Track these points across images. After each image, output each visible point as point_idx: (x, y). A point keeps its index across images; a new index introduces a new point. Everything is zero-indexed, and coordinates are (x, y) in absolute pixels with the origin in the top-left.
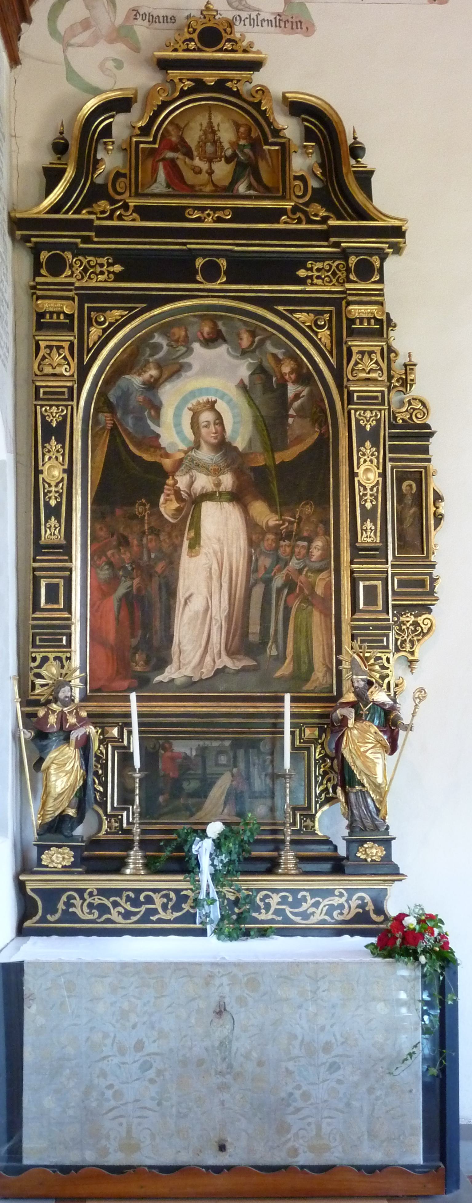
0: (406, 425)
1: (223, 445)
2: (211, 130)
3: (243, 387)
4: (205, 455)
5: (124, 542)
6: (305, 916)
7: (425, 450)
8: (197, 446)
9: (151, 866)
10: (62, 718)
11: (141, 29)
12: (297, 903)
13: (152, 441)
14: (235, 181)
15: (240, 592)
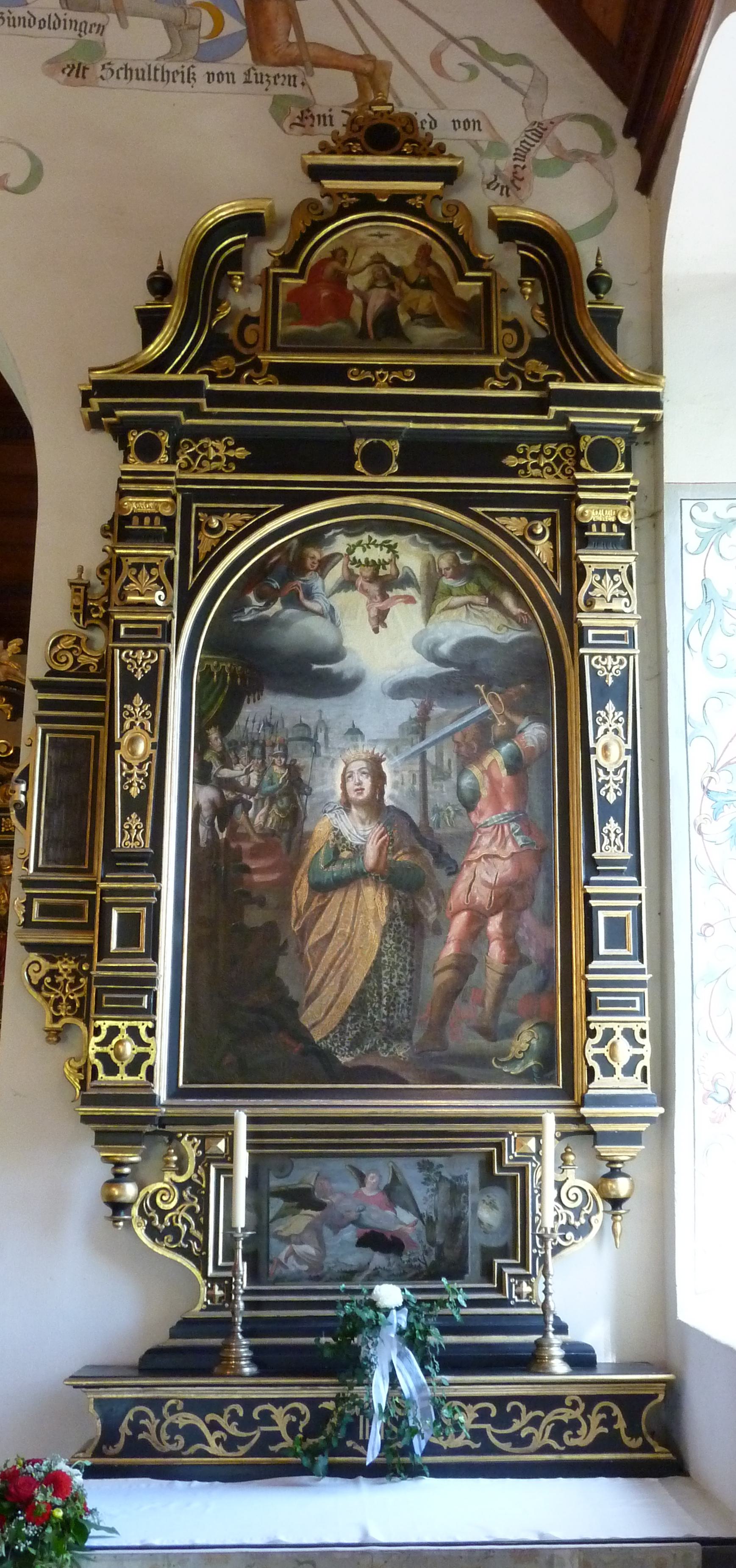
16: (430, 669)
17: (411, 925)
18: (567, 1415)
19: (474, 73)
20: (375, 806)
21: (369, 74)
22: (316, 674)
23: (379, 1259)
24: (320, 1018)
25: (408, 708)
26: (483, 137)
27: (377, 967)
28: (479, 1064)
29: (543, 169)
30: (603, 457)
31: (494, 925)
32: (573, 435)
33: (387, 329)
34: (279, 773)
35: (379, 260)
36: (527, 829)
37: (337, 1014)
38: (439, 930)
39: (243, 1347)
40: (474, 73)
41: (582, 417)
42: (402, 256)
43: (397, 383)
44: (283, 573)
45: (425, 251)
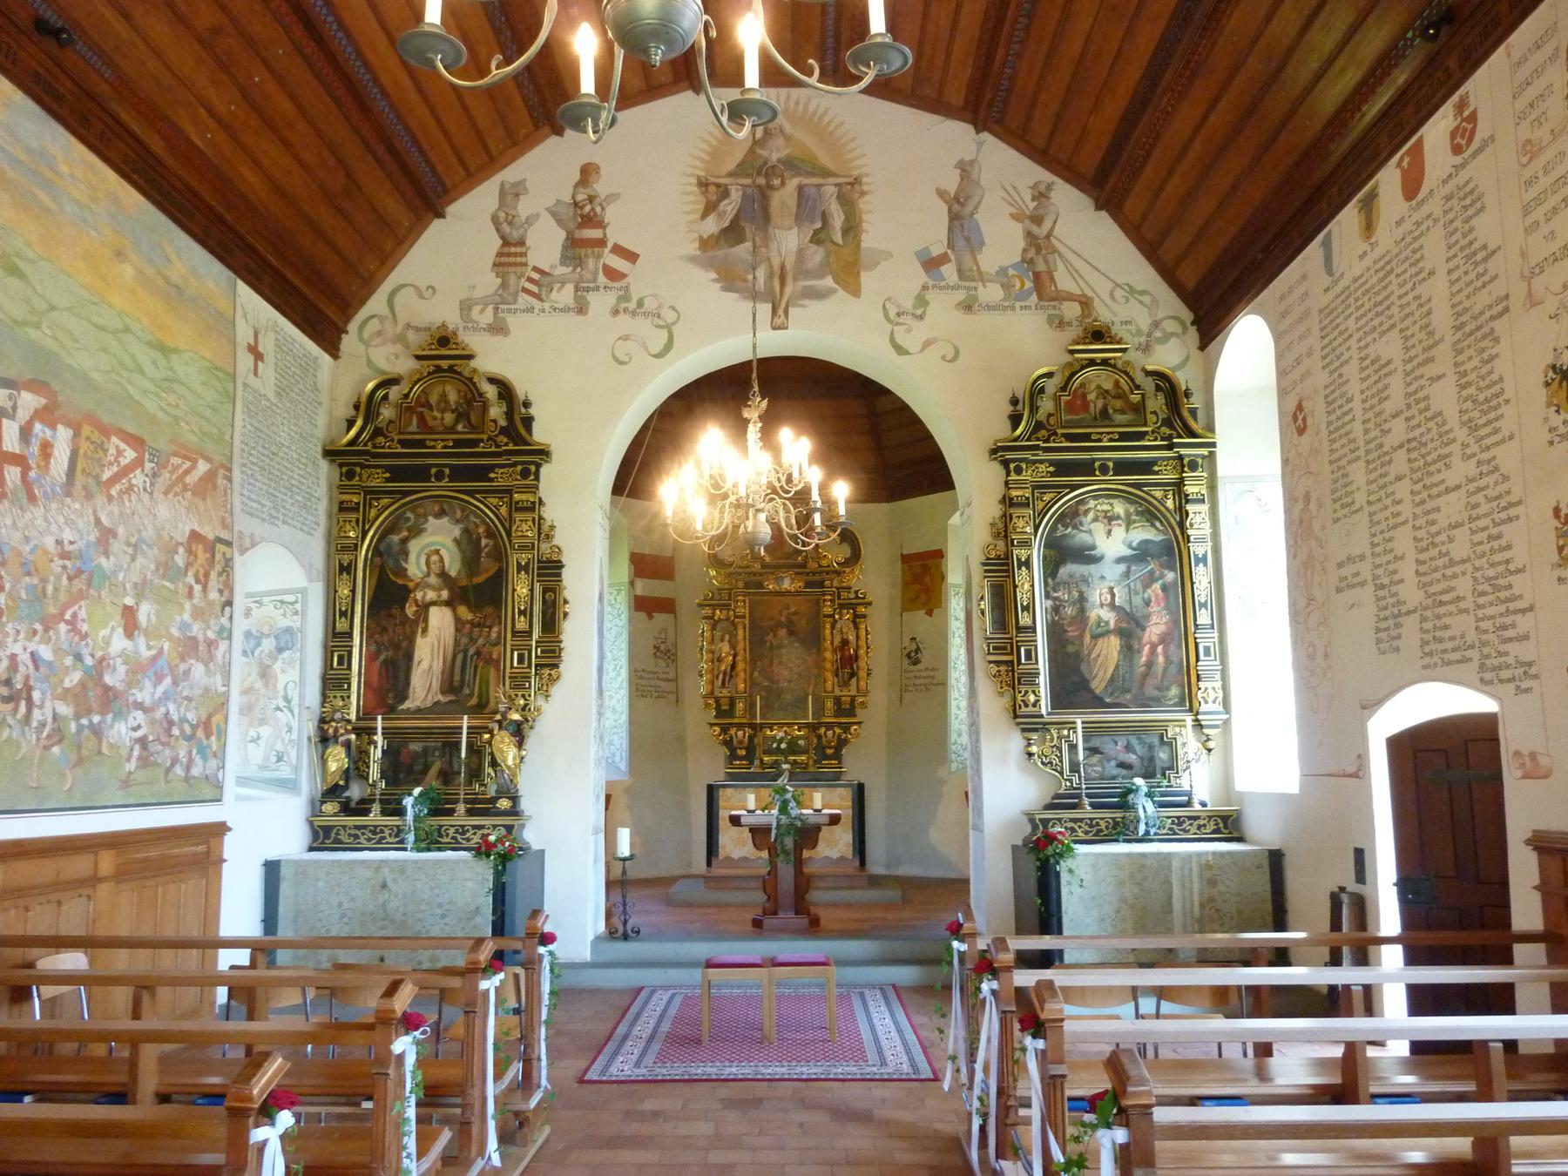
0: (549, 561)
1: (443, 574)
2: (444, 395)
3: (456, 541)
4: (433, 580)
6: (468, 840)
7: (559, 575)
8: (428, 575)
9: (384, 813)
10: (336, 730)
11: (411, 336)
12: (464, 833)
13: (402, 573)
14: (457, 422)
15: (449, 658)
16: (1130, 552)
17: (1129, 650)
18: (1202, 822)
19: (1128, 300)
20: (1112, 606)
21: (1086, 303)
22: (1086, 556)
23: (1124, 772)
24: (1098, 685)
25: (1122, 568)
26: (1133, 328)
27: (1117, 666)
28: (1157, 701)
30: (1193, 466)
31: (1160, 649)
32: (1181, 458)
33: (1104, 414)
34: (1076, 594)
35: (1099, 387)
36: (1170, 613)
37: (1104, 684)
38: (1139, 652)
39: (1086, 801)
40: (1128, 300)
41: (1183, 451)
42: (1108, 385)
43: (1111, 440)
44: (1071, 517)
45: (1117, 382)
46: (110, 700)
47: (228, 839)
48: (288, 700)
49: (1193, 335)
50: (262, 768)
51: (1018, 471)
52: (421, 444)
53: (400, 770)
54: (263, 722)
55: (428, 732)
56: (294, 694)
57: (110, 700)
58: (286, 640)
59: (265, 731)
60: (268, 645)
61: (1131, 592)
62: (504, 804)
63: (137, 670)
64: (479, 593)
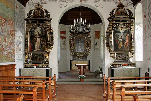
1: (39, 34)
4: (38, 35)
5: (32, 41)
17: (123, 44)
20: (122, 38)
22: (119, 32)
29: (128, 5)
33: (121, 15)
44: (117, 27)
46: (4, 50)
47: (16, 66)
48: (21, 50)
49: (133, 5)
50: (18, 58)
51: (111, 21)
52: (36, 18)
53: (34, 58)
54: (18, 52)
55: (37, 54)
56: (21, 49)
57: (4, 50)
58: (20, 42)
59: (18, 53)
60: (18, 43)
61: (124, 37)
62: (47, 62)
63: (6, 46)
64: (43, 36)
